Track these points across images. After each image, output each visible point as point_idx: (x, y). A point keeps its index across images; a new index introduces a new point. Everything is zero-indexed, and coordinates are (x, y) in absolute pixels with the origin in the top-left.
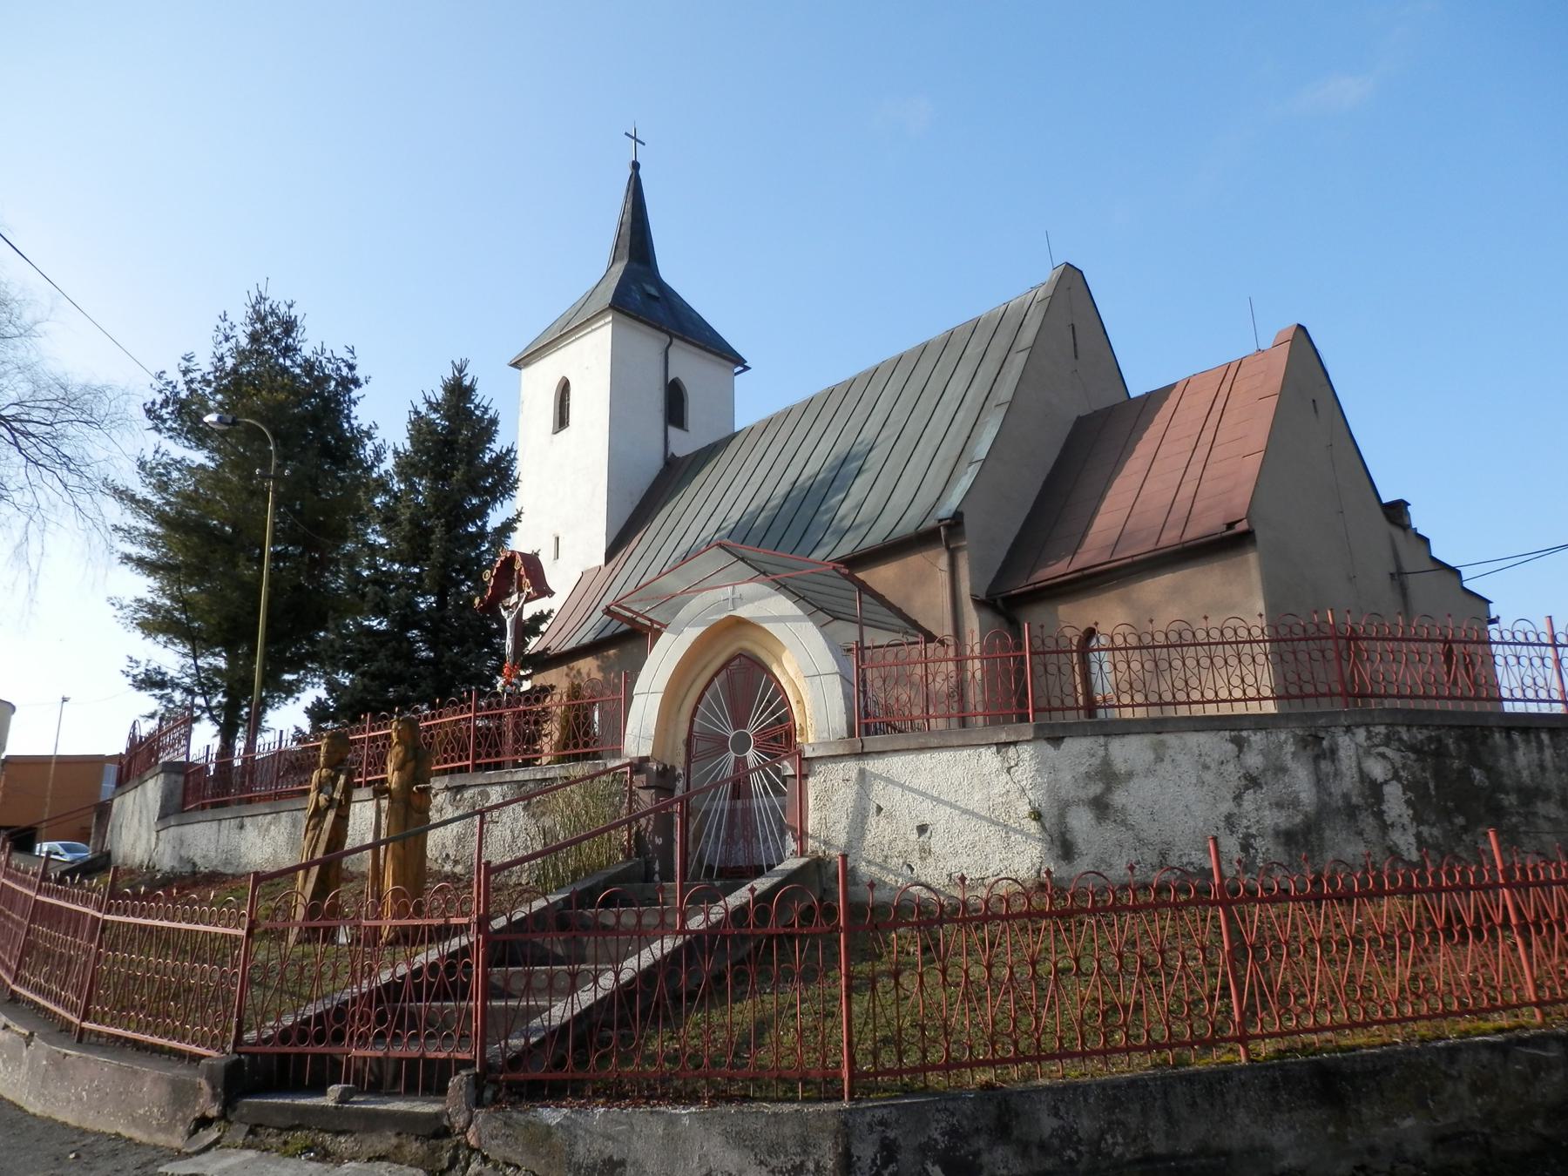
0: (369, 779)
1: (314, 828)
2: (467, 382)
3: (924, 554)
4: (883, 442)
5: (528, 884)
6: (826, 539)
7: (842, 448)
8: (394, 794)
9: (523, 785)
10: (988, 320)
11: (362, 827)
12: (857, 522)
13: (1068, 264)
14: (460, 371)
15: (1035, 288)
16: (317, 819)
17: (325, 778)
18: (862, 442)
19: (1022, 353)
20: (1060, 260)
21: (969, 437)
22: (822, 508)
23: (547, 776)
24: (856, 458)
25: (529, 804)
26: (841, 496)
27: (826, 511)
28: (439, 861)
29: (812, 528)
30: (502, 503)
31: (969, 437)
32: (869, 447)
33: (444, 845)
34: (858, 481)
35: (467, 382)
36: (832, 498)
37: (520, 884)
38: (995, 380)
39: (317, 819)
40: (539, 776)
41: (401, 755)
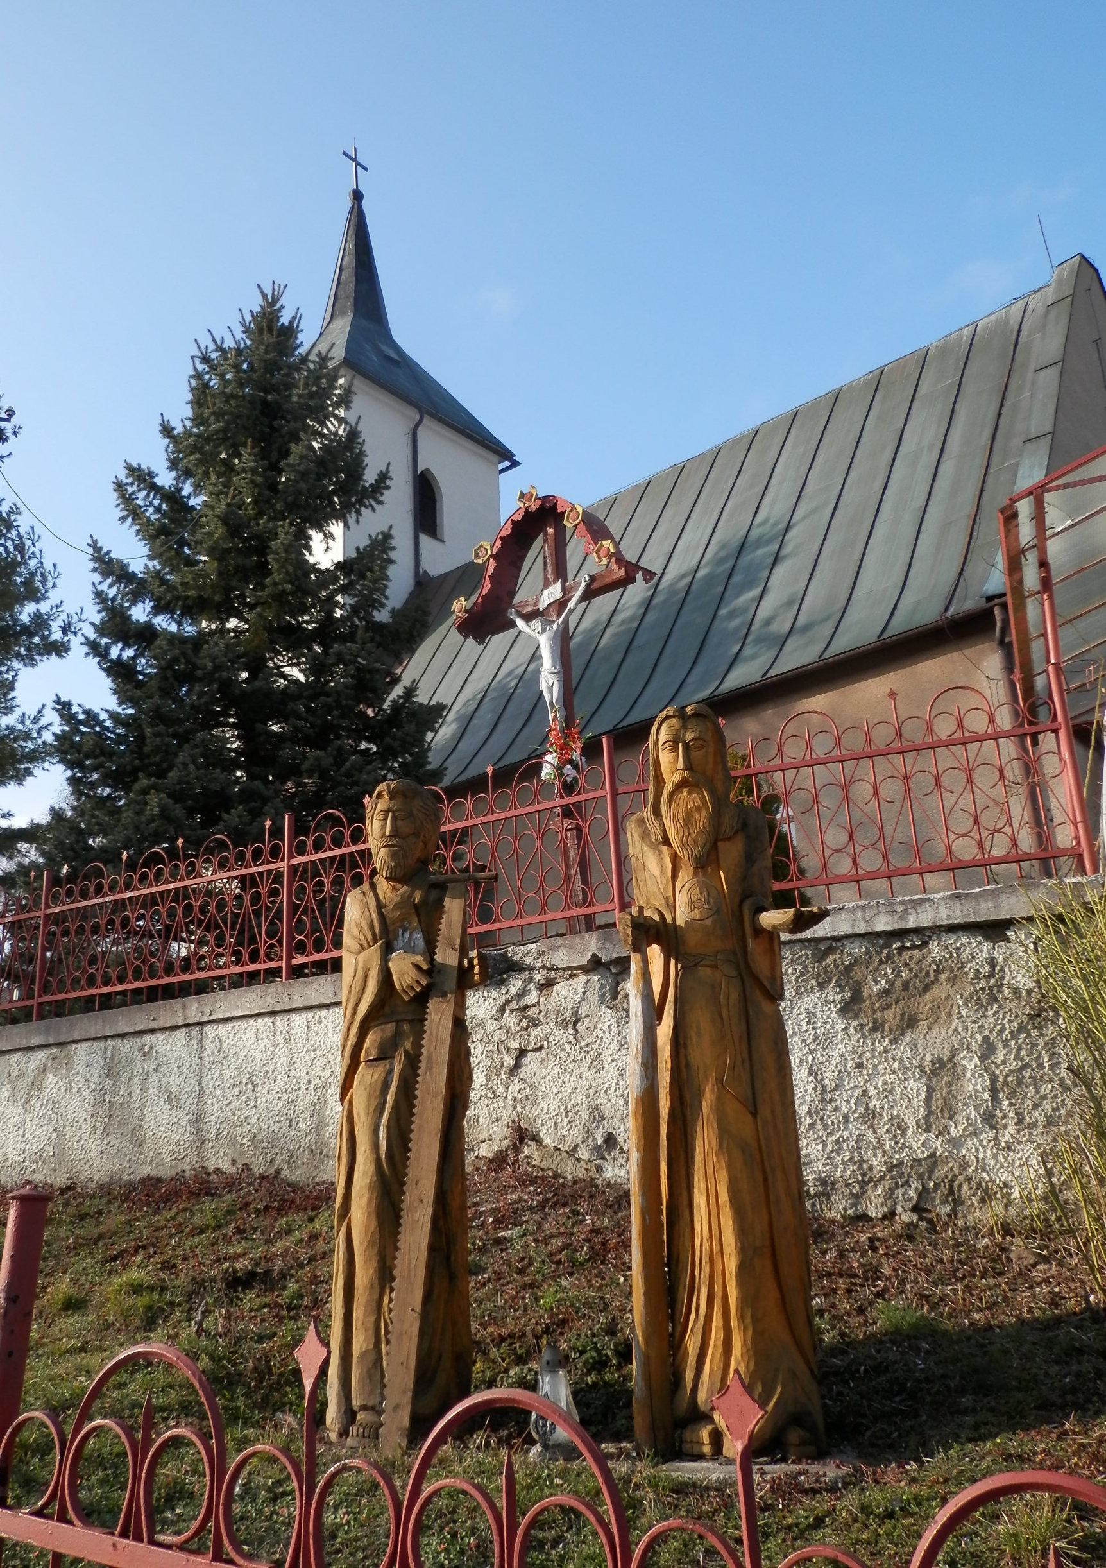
0: (299, 960)
1: (384, 1054)
2: (285, 320)
3: (967, 652)
4: (804, 518)
5: (891, 1215)
6: (748, 651)
7: (730, 531)
8: (693, 940)
9: (830, 950)
10: (944, 350)
11: (317, 1070)
12: (801, 621)
13: (1083, 256)
14: (275, 300)
15: (1021, 298)
16: (390, 1028)
17: (397, 906)
18: (766, 521)
19: (1048, 371)
20: (1066, 249)
21: (982, 491)
22: (723, 612)
23: (912, 922)
24: (760, 542)
25: (857, 997)
26: (756, 592)
27: (732, 615)
28: (584, 1154)
29: (713, 639)
30: (358, 513)
31: (982, 491)
32: (783, 525)
33: (596, 1114)
34: (780, 571)
35: (285, 320)
36: (737, 596)
37: (864, 1217)
38: (999, 414)
39: (390, 1028)
40: (883, 924)
41: (701, 820)
